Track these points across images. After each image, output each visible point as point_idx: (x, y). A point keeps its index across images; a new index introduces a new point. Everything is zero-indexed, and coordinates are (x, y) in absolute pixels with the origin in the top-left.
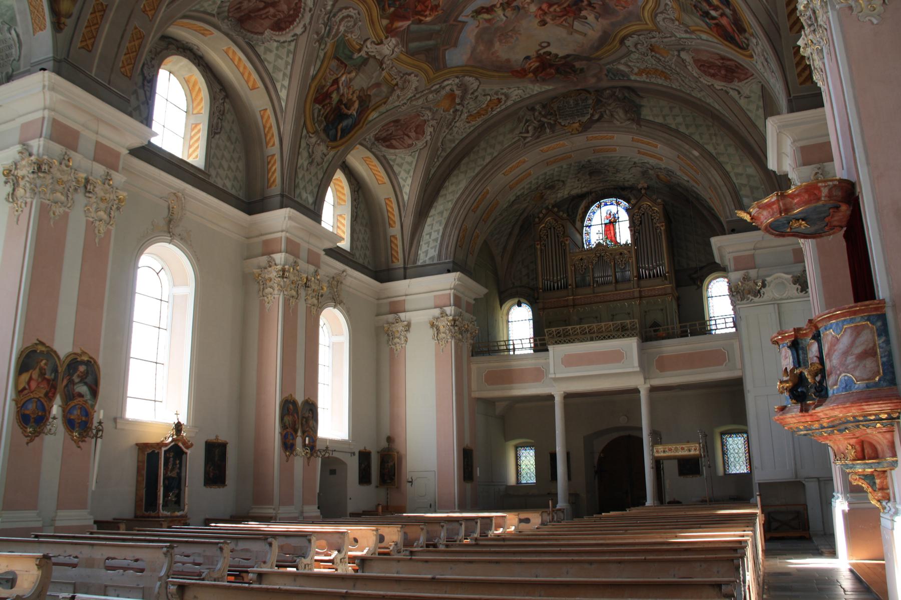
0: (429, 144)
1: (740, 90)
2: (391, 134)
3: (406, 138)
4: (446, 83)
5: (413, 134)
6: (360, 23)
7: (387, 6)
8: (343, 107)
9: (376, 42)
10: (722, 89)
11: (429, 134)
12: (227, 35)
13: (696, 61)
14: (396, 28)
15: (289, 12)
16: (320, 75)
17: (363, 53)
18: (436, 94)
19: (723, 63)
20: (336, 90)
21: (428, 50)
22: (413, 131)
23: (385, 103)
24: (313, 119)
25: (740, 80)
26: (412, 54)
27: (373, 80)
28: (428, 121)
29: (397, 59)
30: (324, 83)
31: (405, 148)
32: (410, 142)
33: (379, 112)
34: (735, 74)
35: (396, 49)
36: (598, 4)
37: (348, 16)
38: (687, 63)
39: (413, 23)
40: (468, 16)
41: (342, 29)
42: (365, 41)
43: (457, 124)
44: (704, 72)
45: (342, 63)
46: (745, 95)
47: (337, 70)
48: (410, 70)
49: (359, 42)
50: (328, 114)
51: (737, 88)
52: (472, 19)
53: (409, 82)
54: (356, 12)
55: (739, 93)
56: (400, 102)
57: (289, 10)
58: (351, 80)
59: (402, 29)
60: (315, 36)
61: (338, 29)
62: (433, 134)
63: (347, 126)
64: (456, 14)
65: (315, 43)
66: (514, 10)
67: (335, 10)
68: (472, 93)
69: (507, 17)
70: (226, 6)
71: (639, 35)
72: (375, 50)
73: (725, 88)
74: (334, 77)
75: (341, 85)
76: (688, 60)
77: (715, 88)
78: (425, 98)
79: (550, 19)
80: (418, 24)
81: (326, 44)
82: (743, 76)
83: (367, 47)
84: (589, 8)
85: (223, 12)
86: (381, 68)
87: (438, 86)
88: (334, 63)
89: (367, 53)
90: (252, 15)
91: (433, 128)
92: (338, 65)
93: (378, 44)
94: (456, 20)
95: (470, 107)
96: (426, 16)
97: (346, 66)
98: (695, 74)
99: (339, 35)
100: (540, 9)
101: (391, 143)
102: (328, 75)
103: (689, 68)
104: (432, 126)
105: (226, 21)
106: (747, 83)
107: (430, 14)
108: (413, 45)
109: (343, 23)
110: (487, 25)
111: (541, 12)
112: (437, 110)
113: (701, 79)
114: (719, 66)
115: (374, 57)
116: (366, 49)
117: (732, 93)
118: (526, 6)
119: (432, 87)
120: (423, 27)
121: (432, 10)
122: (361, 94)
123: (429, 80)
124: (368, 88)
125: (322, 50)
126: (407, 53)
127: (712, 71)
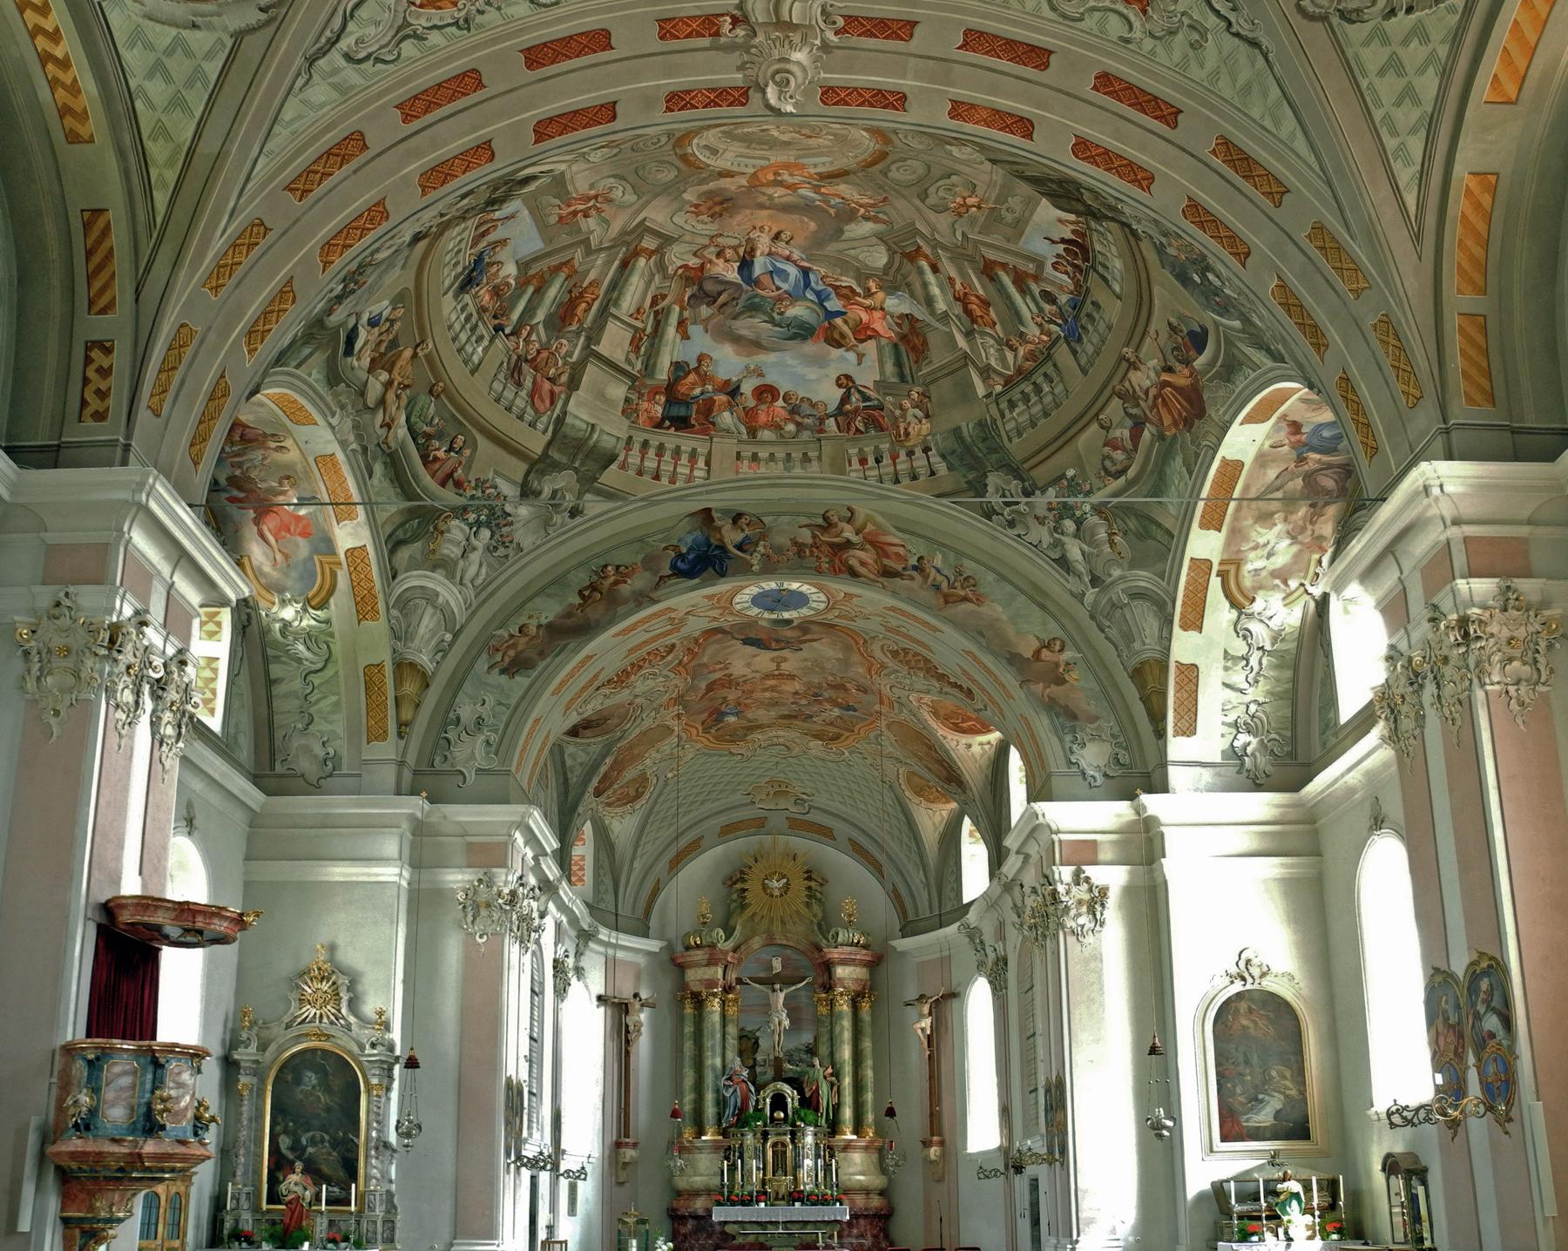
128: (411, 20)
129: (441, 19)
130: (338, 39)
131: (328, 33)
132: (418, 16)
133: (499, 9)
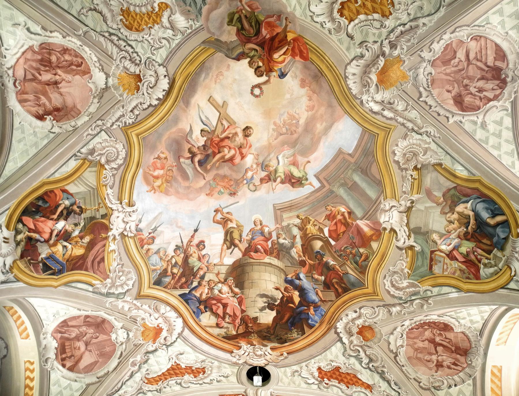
0: (453, 28)
1: (29, 34)
2: (482, 78)
3: (472, 56)
4: (376, 108)
5: (461, 55)
6: (391, 268)
7: (363, 258)
8: (469, 228)
9: (395, 235)
10: (51, 32)
11: (442, 42)
12: (486, 354)
13: (87, 72)
14: (372, 228)
15: (428, 329)
16: (453, 282)
17: (411, 242)
18: (394, 102)
19: (55, 74)
20: (458, 250)
21: (365, 172)
22: (457, 60)
23: (440, 165)
24: (496, 273)
25: (31, 48)
26: (379, 184)
27: (428, 205)
28: (429, 61)
29: (394, 197)
30: (458, 273)
31: (486, 38)
32: (473, 46)
33: (453, 164)
34: (39, 57)
35: (387, 208)
36: (184, 158)
37: (393, 286)
38: (97, 65)
39: (357, 218)
40: (310, 184)
41: (405, 283)
42: (400, 249)
43: (405, 18)
44: (77, 55)
45: (431, 260)
46: (20, 27)
47: (440, 262)
48: (394, 168)
49: (405, 256)
50: (483, 250)
51: (33, 36)
52: (308, 177)
53: (405, 155)
54: (385, 281)
55: (28, 30)
56: (429, 143)
57: (426, 330)
58: (441, 236)
59: (368, 222)
60: (425, 307)
61: (408, 287)
62: (437, 39)
63: (487, 209)
64: (318, 194)
65: (431, 304)
66: (266, 166)
67: (397, 301)
68: (362, 56)
69: (277, 158)
70: (459, 377)
71: (151, 105)
72: (402, 230)
73: (48, 34)
74: (447, 260)
75: (451, 247)
76: (97, 70)
77: (61, 34)
78: (406, 113)
79: (238, 136)
80: (354, 213)
81: (426, 291)
82: (29, 55)
83: (404, 243)
84: (195, 150)
85: (466, 374)
86: (412, 207)
87: (386, 113)
88: (437, 269)
89: (409, 236)
90: (453, 349)
91: (433, 46)
92: (436, 264)
93: (395, 232)
94: (323, 186)
95: (377, 32)
96: (343, 215)
97: (432, 252)
98: (87, 49)
99: (411, 281)
100: (243, 157)
101: (495, 59)
102: (448, 270)
103: (95, 59)
104: (431, 51)
105: (473, 364)
106: (22, 46)
107: (338, 214)
108: (372, 194)
109: (401, 286)
110: (301, 159)
111: (244, 151)
112: (410, 70)
113: (79, 43)
114: (59, 67)
115: (407, 225)
116: (407, 241)
117: (37, 29)
118: (255, 166)
119: (391, 119)
120: (352, 205)
121: (334, 217)
122: (447, 210)
123: (388, 130)
124: (438, 204)
125: (432, 293)
126: (383, 191)
127: (67, 57)
128: (143, 387)
129: (152, 388)
130: (119, 390)
131: (116, 388)
132: (145, 387)
133: (171, 387)
